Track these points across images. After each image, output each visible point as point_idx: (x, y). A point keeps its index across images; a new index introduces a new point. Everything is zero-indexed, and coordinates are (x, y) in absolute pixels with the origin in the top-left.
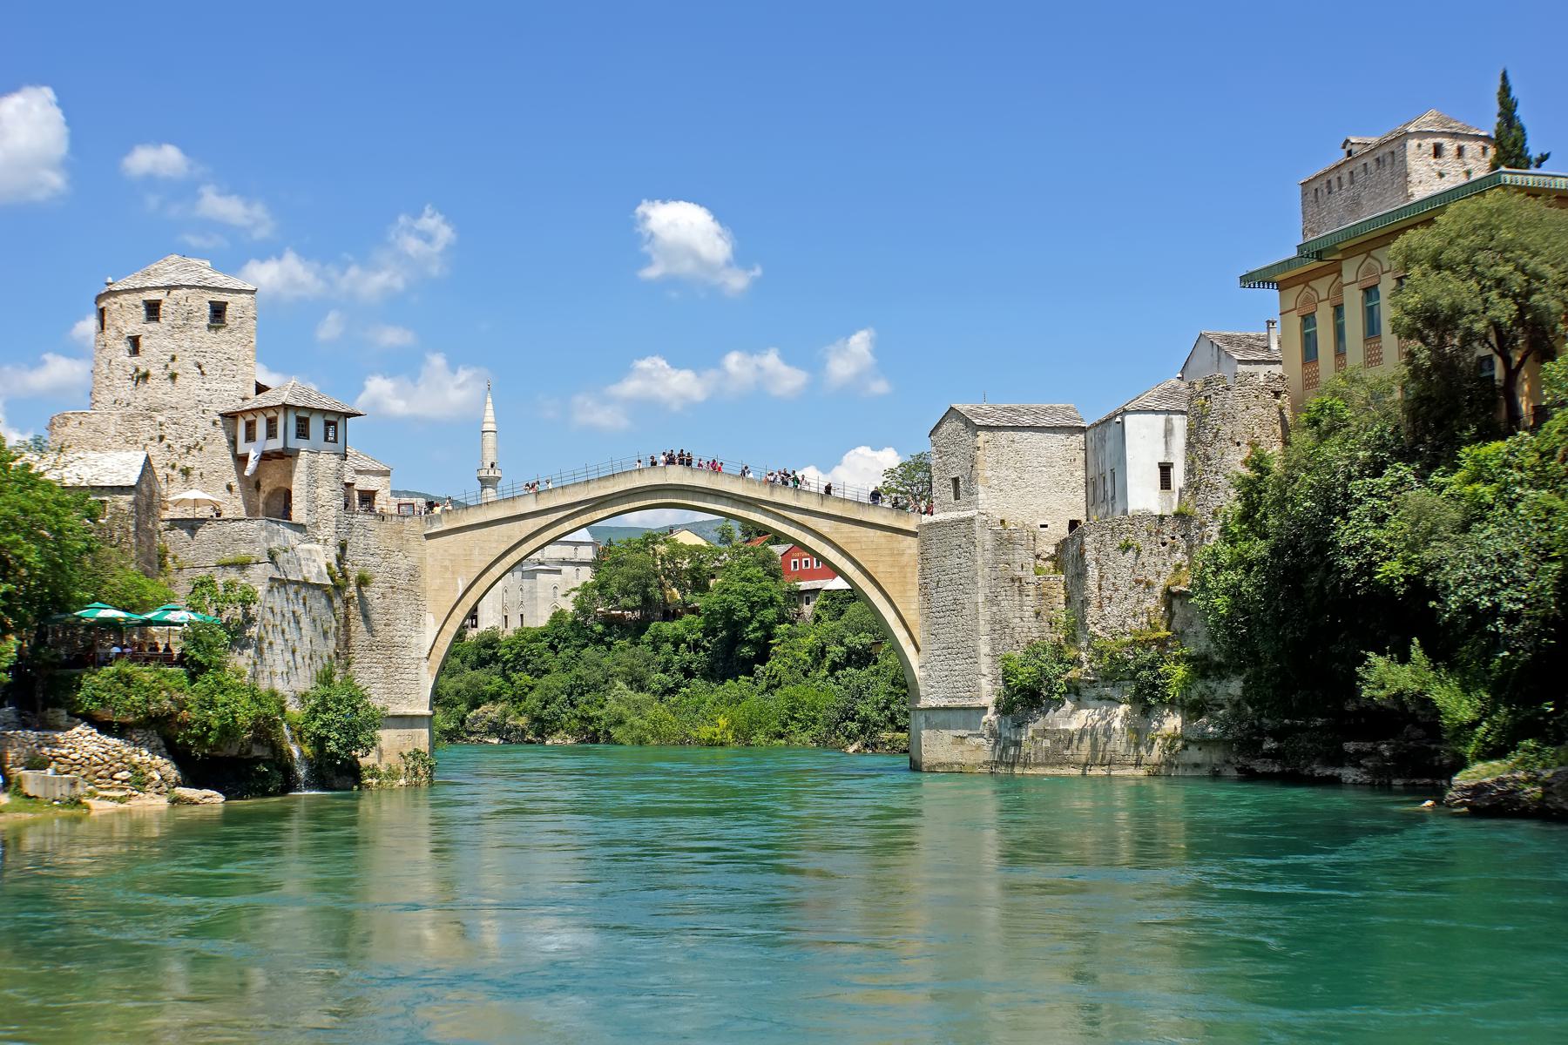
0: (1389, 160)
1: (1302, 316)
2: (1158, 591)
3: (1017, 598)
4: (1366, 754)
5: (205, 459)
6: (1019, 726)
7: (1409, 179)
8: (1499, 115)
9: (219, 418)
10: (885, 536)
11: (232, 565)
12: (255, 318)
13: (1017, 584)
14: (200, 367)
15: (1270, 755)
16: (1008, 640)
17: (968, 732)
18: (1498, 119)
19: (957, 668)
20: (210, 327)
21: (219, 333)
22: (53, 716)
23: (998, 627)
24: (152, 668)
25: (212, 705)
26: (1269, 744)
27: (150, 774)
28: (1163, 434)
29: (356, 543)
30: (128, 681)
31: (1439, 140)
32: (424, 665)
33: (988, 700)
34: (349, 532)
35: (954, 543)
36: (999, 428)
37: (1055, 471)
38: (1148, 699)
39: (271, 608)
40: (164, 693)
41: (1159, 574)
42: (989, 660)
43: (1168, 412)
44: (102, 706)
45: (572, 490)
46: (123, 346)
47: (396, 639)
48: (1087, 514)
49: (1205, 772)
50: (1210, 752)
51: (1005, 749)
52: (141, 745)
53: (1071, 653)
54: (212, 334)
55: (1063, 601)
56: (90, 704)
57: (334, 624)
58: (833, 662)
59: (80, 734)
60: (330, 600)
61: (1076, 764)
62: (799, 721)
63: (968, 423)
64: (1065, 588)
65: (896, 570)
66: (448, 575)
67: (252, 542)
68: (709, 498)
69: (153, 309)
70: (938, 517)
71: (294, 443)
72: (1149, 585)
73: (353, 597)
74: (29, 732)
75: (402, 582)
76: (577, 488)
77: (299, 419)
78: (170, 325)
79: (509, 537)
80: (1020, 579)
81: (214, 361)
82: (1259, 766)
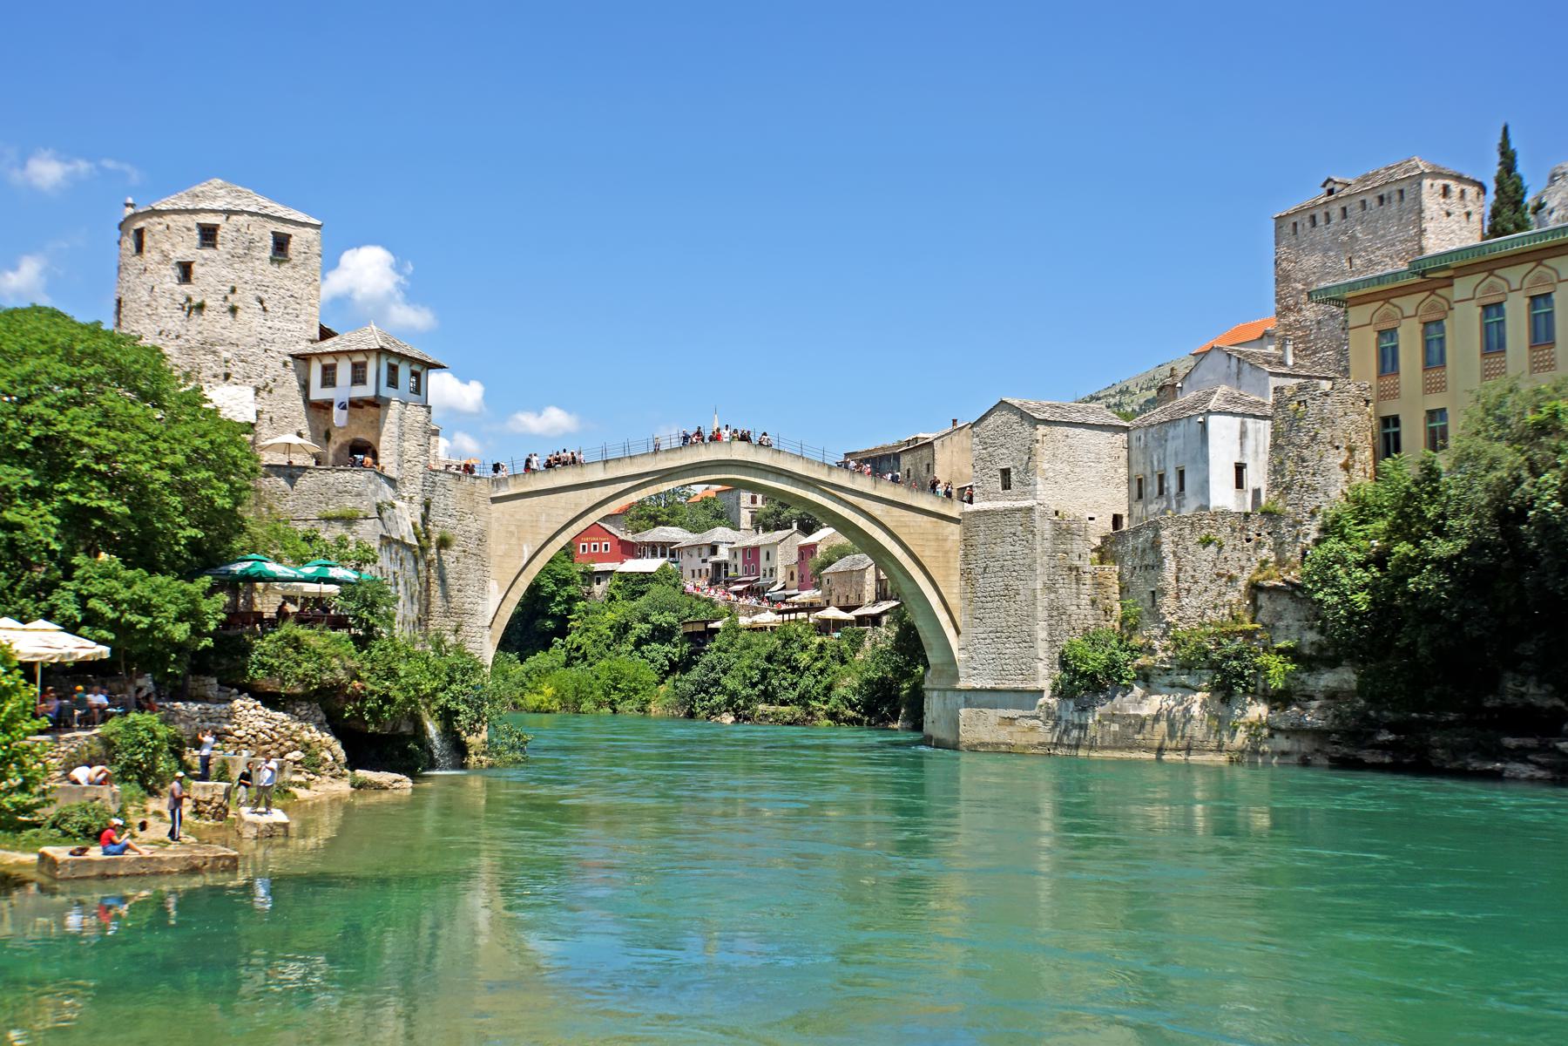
0: (1396, 197)
1: (1379, 332)
2: (1242, 584)
3: (1074, 586)
4: (1532, 750)
5: (274, 403)
6: (1084, 710)
7: (1423, 215)
8: (1500, 164)
9: (289, 359)
10: (931, 522)
11: (337, 519)
12: (320, 256)
13: (1074, 573)
14: (261, 302)
15: (1384, 747)
16: (1065, 627)
17: (1020, 712)
18: (1499, 168)
19: (1007, 651)
20: (272, 260)
21: (282, 268)
22: (196, 685)
23: (1055, 613)
24: (316, 631)
25: (392, 674)
26: (1385, 736)
27: (322, 754)
28: (1238, 436)
29: (439, 503)
30: (297, 644)
31: (1447, 182)
32: (487, 633)
33: (1045, 684)
34: (432, 492)
35: (1008, 531)
36: (1056, 423)
37: (1101, 467)
38: (1228, 687)
39: (381, 568)
40: (335, 662)
41: (1242, 568)
42: (1046, 645)
43: (1243, 415)
44: (268, 675)
45: (640, 460)
46: (171, 272)
47: (467, 606)
48: (1130, 509)
49: (1295, 759)
50: (1299, 741)
51: (1066, 731)
52: (306, 720)
53: (1137, 641)
54: (274, 268)
55: (1117, 591)
56: (255, 672)
57: (418, 587)
58: (639, 638)
59: (244, 707)
60: (416, 562)
61: (1148, 749)
62: (620, 690)
63: (1024, 416)
64: (1120, 578)
65: (940, 554)
66: (514, 541)
67: (359, 495)
68: (770, 476)
69: (208, 235)
70: (976, 506)
71: (386, 392)
72: (1232, 579)
73: (433, 560)
74: (191, 704)
75: (472, 547)
76: (645, 459)
77: (355, 366)
78: (229, 253)
79: (576, 505)
80: (1077, 569)
81: (277, 297)
82: (1368, 756)
